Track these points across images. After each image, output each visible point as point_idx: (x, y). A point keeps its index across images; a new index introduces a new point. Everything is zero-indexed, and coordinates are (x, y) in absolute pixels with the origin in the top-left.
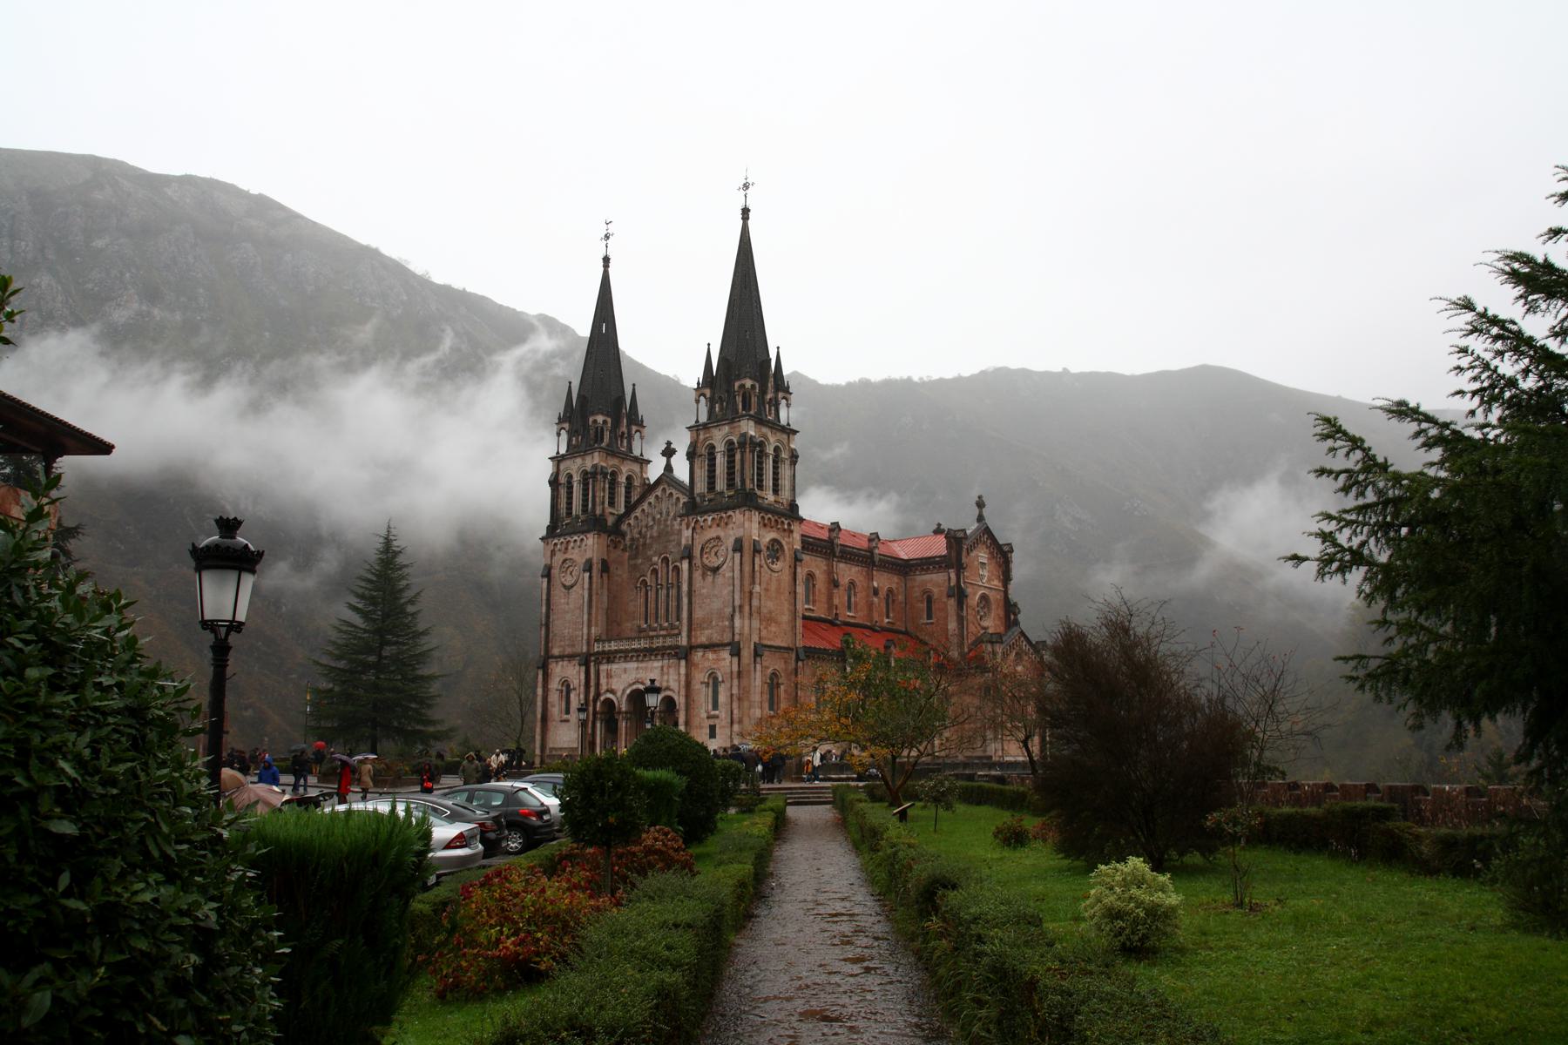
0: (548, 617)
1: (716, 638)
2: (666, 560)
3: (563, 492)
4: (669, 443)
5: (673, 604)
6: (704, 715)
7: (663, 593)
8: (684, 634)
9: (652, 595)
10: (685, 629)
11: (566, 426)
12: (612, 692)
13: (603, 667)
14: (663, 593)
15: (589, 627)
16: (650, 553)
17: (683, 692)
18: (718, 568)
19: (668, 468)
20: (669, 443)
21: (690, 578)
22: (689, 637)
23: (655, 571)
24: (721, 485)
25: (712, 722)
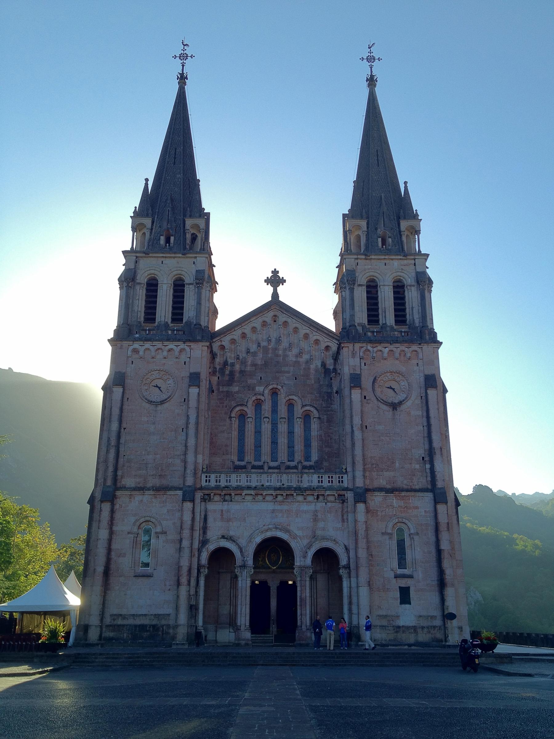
0: (119, 437)
1: (402, 482)
2: (274, 393)
3: (141, 293)
4: (275, 272)
5: (283, 441)
6: (392, 575)
7: (266, 427)
8: (359, 474)
9: (250, 427)
10: (359, 467)
11: (148, 222)
12: (231, 539)
13: (211, 506)
14: (266, 427)
15: (196, 453)
16: (250, 381)
17: (362, 544)
18: (400, 403)
19: (275, 295)
20: (275, 272)
21: (362, 412)
22: (364, 476)
23: (258, 404)
24: (388, 316)
25: (403, 583)
